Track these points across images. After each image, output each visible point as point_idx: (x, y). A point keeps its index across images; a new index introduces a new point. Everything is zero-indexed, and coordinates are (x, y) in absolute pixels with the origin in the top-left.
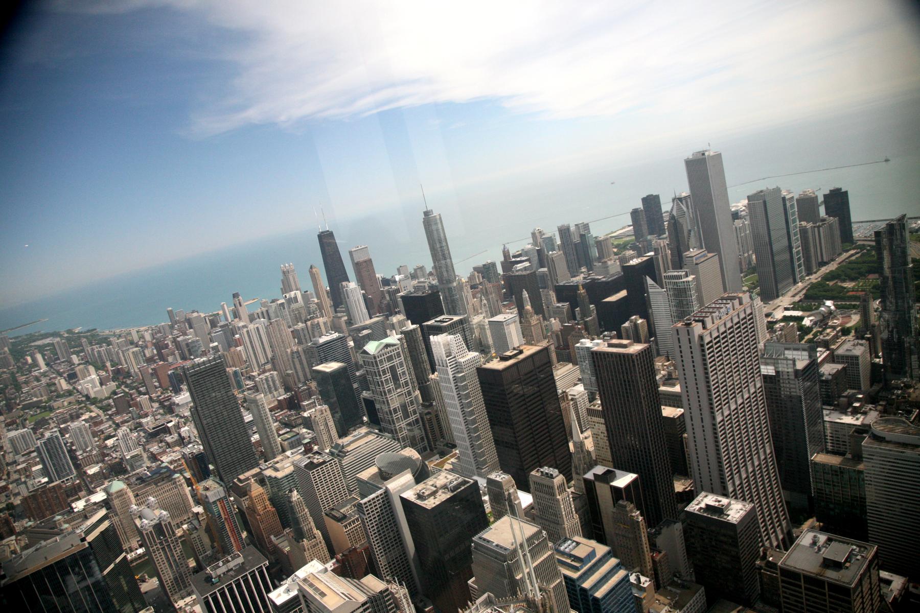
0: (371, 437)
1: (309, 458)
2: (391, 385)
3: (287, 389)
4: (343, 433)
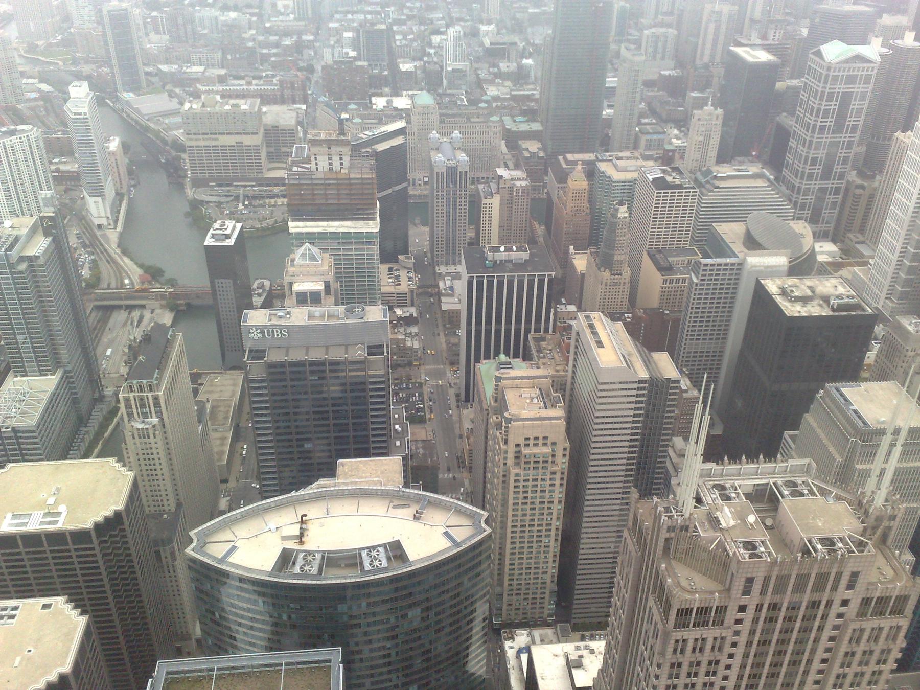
0: (760, 183)
1: (664, 171)
2: (830, 122)
3: (680, 64)
4: (722, 159)
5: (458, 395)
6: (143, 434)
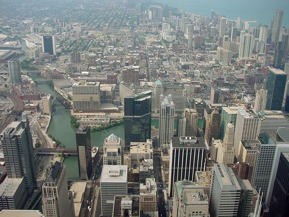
0: (282, 117)
5: (167, 194)
6: (49, 202)
